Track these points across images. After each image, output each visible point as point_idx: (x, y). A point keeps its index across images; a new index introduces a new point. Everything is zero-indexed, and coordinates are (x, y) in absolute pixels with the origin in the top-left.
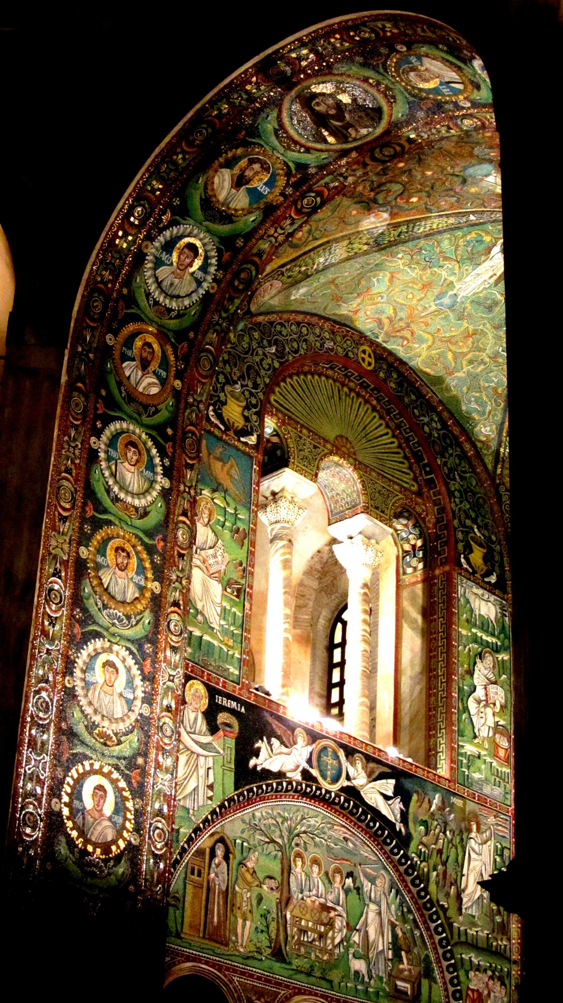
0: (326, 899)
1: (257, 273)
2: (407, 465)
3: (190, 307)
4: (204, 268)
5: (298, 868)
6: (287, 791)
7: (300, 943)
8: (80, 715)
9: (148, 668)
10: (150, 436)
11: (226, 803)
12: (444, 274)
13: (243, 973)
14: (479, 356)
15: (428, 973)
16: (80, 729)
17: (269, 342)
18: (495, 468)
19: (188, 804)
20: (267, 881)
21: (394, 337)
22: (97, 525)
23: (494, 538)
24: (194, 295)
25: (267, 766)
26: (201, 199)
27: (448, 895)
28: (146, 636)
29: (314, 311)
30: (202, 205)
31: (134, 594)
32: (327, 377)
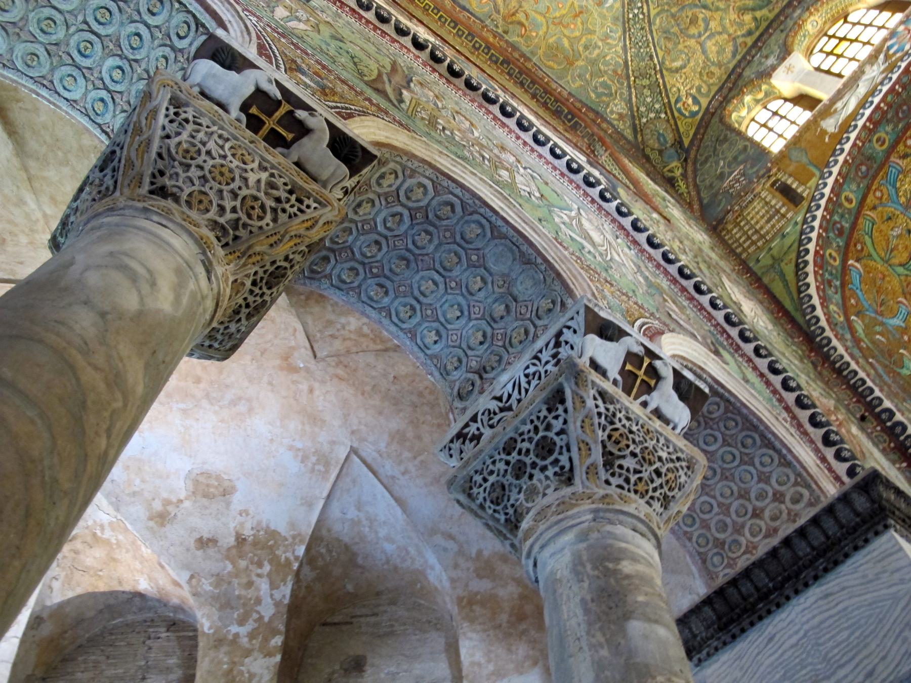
18: (636, 137)
21: (512, 23)
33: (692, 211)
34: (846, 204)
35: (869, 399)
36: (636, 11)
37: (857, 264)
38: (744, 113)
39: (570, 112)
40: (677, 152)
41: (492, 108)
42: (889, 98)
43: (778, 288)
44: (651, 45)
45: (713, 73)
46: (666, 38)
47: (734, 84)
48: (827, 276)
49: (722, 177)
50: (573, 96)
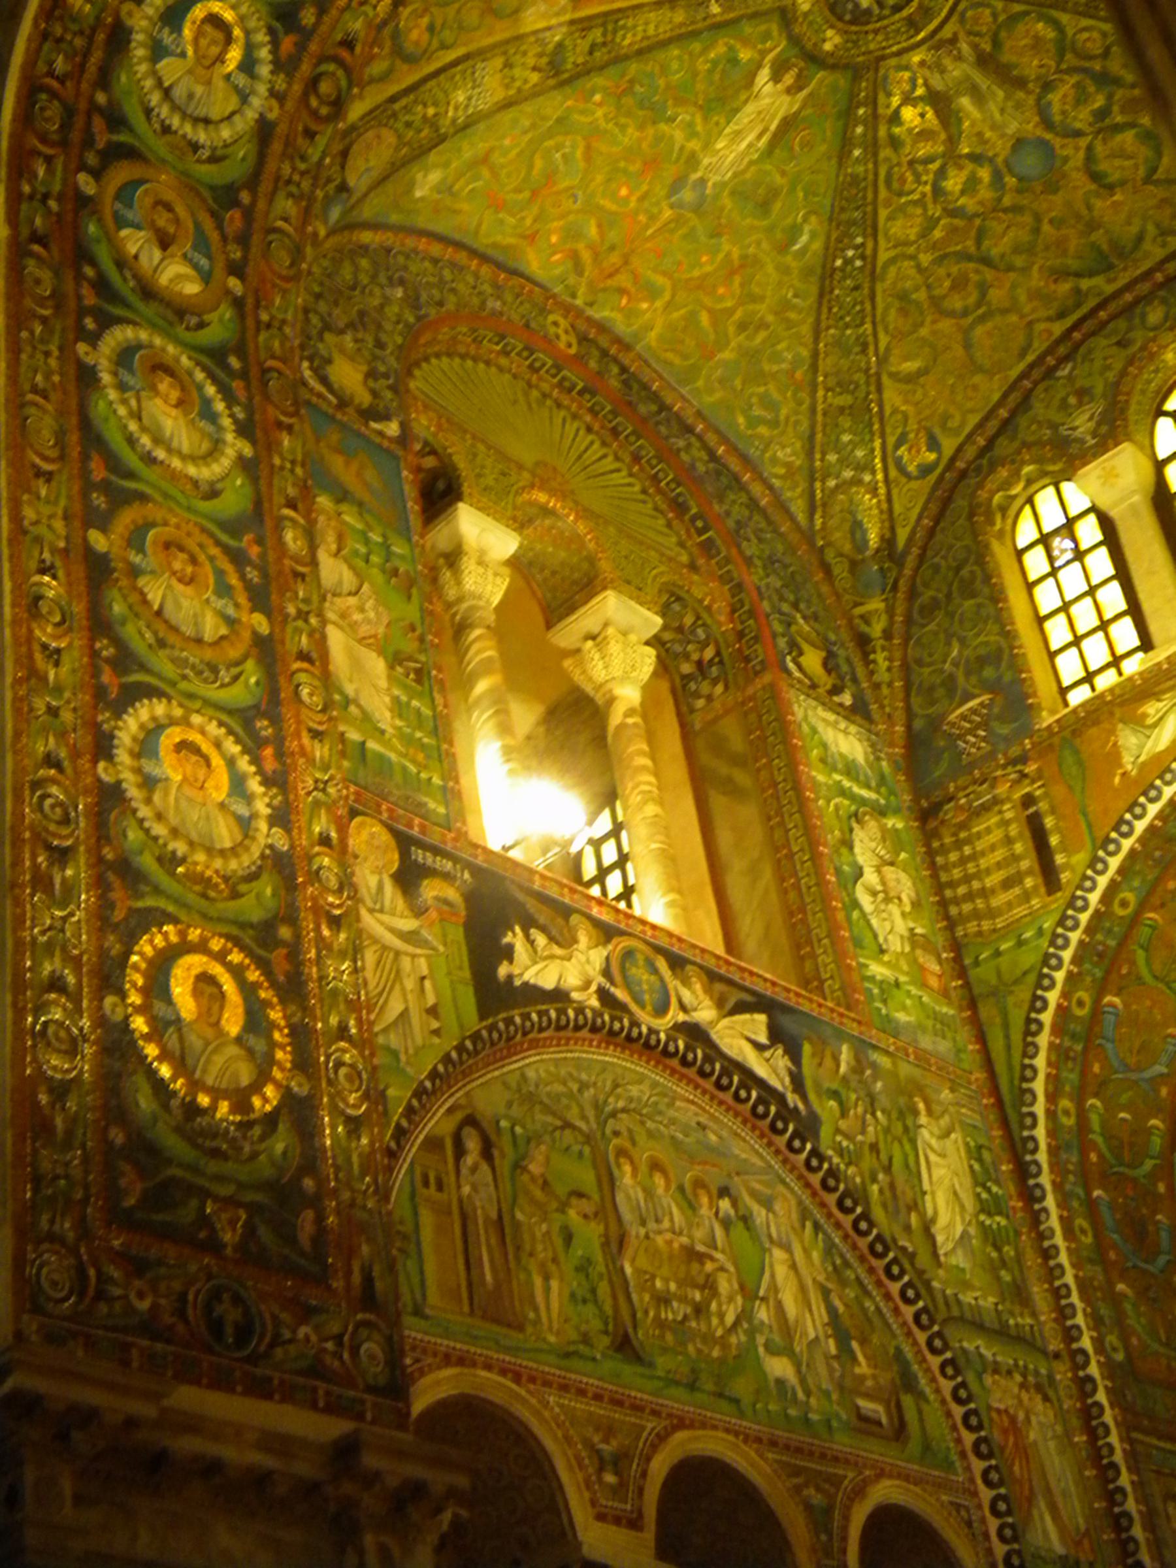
0: (690, 1237)
1: (350, 86)
2: (661, 522)
4: (248, 65)
5: (626, 1177)
6: (577, 1028)
7: (661, 1324)
8: (141, 835)
9: (270, 765)
10: (198, 364)
11: (468, 1044)
12: (679, 136)
13: (564, 1388)
15: (908, 1382)
16: (147, 862)
17: (390, 279)
19: (394, 1040)
20: (574, 1201)
21: (605, 290)
22: (121, 499)
23: (832, 637)
24: (237, 118)
25: (530, 976)
27: (907, 1228)
28: (256, 707)
29: (457, 237)
31: (217, 628)
32: (501, 369)
33: (892, 745)
34: (1121, 912)
35: (1069, 1323)
36: (850, 253)
37: (1116, 1000)
38: (1017, 489)
41: (668, 1061)
45: (975, 388)
47: (1014, 413)
48: (1067, 1043)
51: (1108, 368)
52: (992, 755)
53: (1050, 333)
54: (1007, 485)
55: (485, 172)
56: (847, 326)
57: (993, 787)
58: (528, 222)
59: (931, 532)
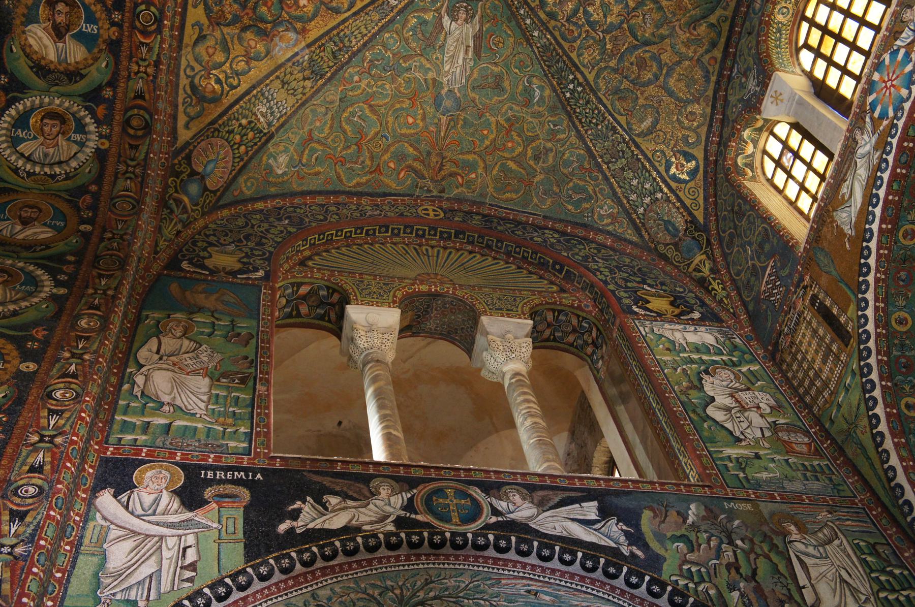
1: (151, 116)
3: (80, 167)
14: (538, 147)
18: (641, 236)
21: (443, 179)
24: (79, 155)
26: (31, 68)
29: (330, 188)
30: (36, 73)
33: (742, 328)
36: (571, 86)
38: (750, 149)
39: (555, 263)
40: (694, 238)
41: (486, 553)
42: (895, 187)
43: (866, 470)
44: (606, 115)
45: (691, 113)
46: (620, 99)
47: (724, 114)
49: (756, 273)
50: (550, 218)
51: (751, 48)
52: (788, 291)
53: (715, 59)
54: (740, 151)
55: (317, 146)
56: (598, 124)
57: (795, 309)
58: (368, 162)
59: (715, 203)
